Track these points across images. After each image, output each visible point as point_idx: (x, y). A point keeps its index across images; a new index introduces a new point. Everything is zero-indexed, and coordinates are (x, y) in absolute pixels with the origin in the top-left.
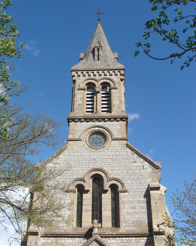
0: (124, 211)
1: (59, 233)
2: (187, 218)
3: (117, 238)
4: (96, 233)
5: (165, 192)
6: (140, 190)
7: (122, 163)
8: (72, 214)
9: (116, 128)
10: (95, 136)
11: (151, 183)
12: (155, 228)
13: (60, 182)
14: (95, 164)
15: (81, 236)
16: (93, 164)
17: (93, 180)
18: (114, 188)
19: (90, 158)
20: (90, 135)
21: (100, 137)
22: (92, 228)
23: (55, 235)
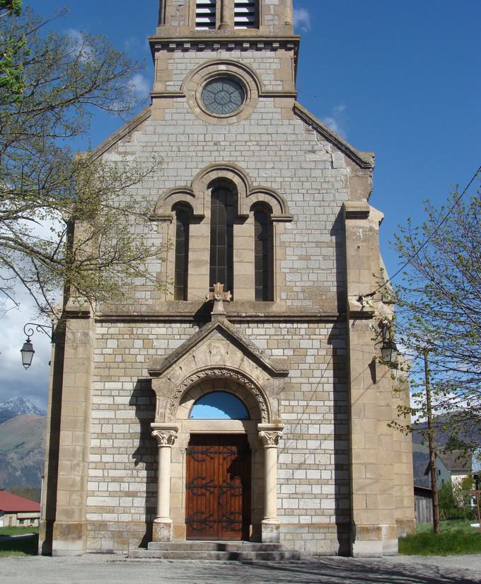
0: (283, 264)
1: (135, 314)
2: (428, 282)
3: (266, 325)
4: (219, 313)
5: (380, 223)
6: (323, 218)
7: (283, 153)
8: (164, 270)
9: (270, 68)
10: (218, 86)
11: (349, 202)
12: (353, 303)
13: (139, 199)
14: (217, 153)
15: (187, 319)
16: (201, 149)
17: (212, 192)
18: (262, 211)
19: (207, 140)
20: (205, 82)
21: (230, 87)
22: (210, 301)
23: (128, 318)
